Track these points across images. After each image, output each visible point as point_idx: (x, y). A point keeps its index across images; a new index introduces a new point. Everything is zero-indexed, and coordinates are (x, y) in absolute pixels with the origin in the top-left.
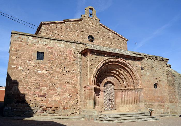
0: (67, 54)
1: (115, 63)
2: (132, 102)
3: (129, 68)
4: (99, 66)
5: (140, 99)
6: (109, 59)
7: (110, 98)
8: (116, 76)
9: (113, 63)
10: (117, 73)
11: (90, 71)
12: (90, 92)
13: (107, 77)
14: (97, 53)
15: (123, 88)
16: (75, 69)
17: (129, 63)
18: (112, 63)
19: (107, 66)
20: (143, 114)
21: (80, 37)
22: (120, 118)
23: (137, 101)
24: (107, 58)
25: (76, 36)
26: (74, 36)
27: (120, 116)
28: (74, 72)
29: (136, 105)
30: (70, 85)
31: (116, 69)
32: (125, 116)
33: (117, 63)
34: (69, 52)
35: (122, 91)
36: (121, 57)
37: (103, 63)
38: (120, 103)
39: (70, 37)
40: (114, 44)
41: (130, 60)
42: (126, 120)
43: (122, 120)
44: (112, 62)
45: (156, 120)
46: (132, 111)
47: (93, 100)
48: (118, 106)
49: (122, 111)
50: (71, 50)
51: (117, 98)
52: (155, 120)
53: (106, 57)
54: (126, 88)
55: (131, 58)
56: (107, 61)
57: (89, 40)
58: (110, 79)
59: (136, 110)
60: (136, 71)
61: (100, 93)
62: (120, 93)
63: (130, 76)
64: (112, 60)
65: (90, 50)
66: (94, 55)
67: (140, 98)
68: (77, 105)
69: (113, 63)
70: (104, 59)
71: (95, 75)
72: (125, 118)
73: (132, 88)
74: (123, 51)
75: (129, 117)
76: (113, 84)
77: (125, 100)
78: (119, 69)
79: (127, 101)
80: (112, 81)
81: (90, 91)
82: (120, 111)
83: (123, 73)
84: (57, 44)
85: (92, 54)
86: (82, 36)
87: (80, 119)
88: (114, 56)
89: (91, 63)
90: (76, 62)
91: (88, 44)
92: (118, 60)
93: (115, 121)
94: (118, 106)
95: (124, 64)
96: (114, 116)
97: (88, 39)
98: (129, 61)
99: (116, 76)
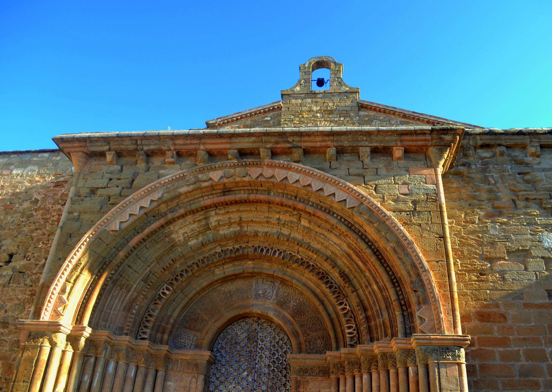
0: (39, 198)
30: (10, 333)
34: (52, 188)
50: (62, 179)
65: (76, 144)
84: (12, 167)
89: (77, 207)
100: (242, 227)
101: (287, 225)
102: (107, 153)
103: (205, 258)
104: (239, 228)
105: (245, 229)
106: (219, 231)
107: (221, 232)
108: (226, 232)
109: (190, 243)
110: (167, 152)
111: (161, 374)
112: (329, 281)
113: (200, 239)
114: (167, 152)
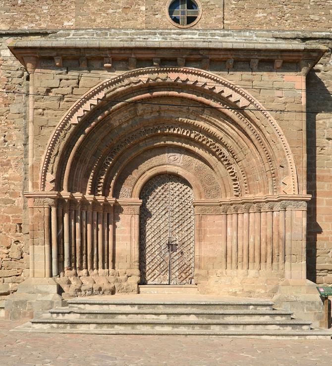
1: (165, 93)
2: (257, 254)
3: (234, 106)
4: (76, 110)
5: (288, 243)
6: (128, 77)
7: (177, 238)
8: (196, 150)
9: (155, 94)
10: (175, 132)
11: (38, 135)
12: (36, 217)
13: (155, 156)
14: (64, 59)
15: (229, 198)
16: (10, 136)
17: (233, 84)
18: (148, 95)
19: (136, 110)
20: (264, 308)
21: (138, 11)
22: (124, 317)
23: (276, 251)
24: (118, 74)
25: (120, 10)
26: (111, 11)
27: (135, 309)
28: (8, 148)
29: (269, 270)
31: (185, 120)
32: (161, 309)
33: (176, 93)
35: (225, 209)
36: (188, 62)
37: (96, 97)
38: (216, 258)
39: (95, 21)
40: (293, 15)
41: (243, 69)
42: (138, 327)
43: (116, 326)
44: (150, 87)
45: (303, 338)
46: (250, 292)
47: (47, 246)
48: (203, 272)
49: (214, 292)
51: (200, 240)
52: (297, 338)
53: (109, 69)
54: (238, 199)
55: (248, 61)
56: (118, 90)
57: (176, 20)
58: (173, 162)
59: (263, 291)
60: (272, 118)
61: (119, 219)
62: (219, 220)
63: (251, 144)
64: (144, 78)
66: (54, 71)
67: (288, 238)
68: (18, 264)
69: (155, 94)
70: (99, 81)
71: (60, 146)
72: (148, 316)
73: (260, 196)
74: (225, 36)
75: (172, 317)
76: (185, 182)
77: (234, 249)
78: (197, 117)
79: (240, 253)
80: (181, 172)
81: (35, 214)
82: (208, 293)
83: (219, 134)
85: (45, 68)
86: (143, 8)
87: (155, 326)
88: (149, 62)
90: (14, 108)
91: (61, 32)
92: (173, 77)
93: (82, 328)
94: (203, 272)
95: (210, 94)
96: (105, 307)
97: (171, 13)
98: (235, 78)
99: (196, 150)
100: (160, 114)
101: (194, 113)
102: (55, 58)
103: (133, 135)
104: (158, 114)
105: (162, 115)
106: (143, 116)
107: (145, 117)
108: (149, 117)
109: (123, 126)
110: (105, 59)
111: (111, 216)
112: (222, 153)
113: (130, 123)
114: (105, 59)
